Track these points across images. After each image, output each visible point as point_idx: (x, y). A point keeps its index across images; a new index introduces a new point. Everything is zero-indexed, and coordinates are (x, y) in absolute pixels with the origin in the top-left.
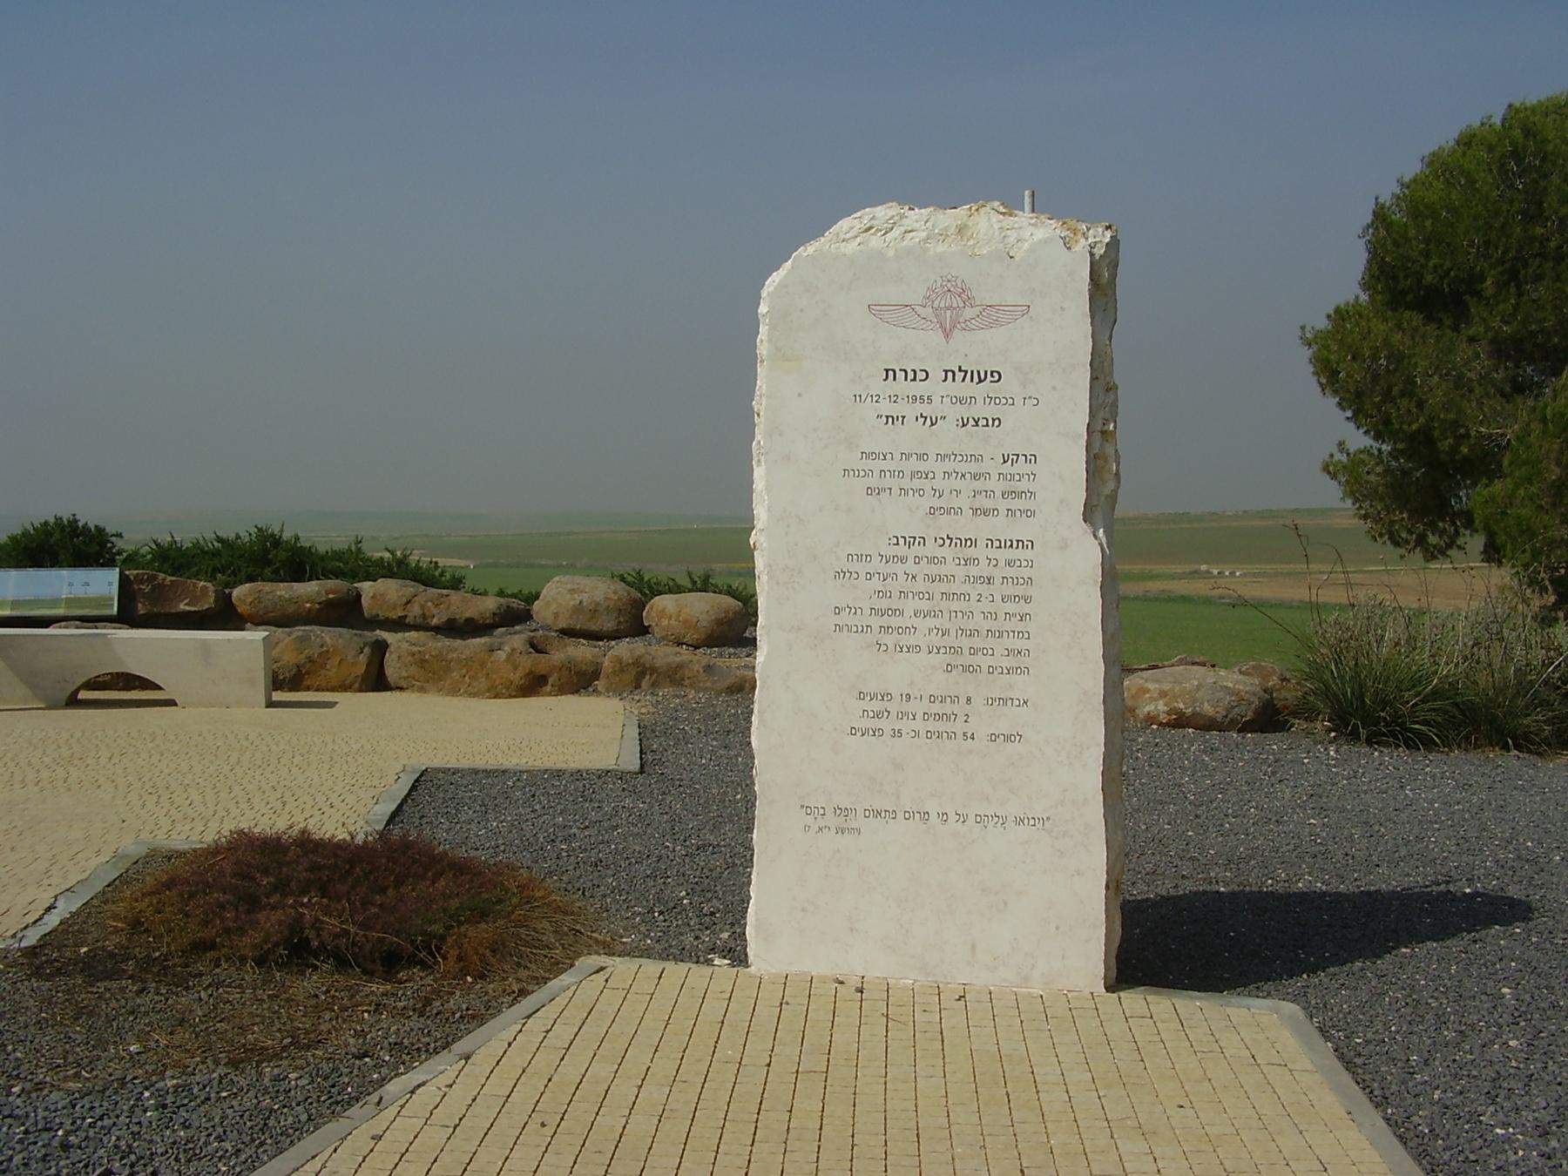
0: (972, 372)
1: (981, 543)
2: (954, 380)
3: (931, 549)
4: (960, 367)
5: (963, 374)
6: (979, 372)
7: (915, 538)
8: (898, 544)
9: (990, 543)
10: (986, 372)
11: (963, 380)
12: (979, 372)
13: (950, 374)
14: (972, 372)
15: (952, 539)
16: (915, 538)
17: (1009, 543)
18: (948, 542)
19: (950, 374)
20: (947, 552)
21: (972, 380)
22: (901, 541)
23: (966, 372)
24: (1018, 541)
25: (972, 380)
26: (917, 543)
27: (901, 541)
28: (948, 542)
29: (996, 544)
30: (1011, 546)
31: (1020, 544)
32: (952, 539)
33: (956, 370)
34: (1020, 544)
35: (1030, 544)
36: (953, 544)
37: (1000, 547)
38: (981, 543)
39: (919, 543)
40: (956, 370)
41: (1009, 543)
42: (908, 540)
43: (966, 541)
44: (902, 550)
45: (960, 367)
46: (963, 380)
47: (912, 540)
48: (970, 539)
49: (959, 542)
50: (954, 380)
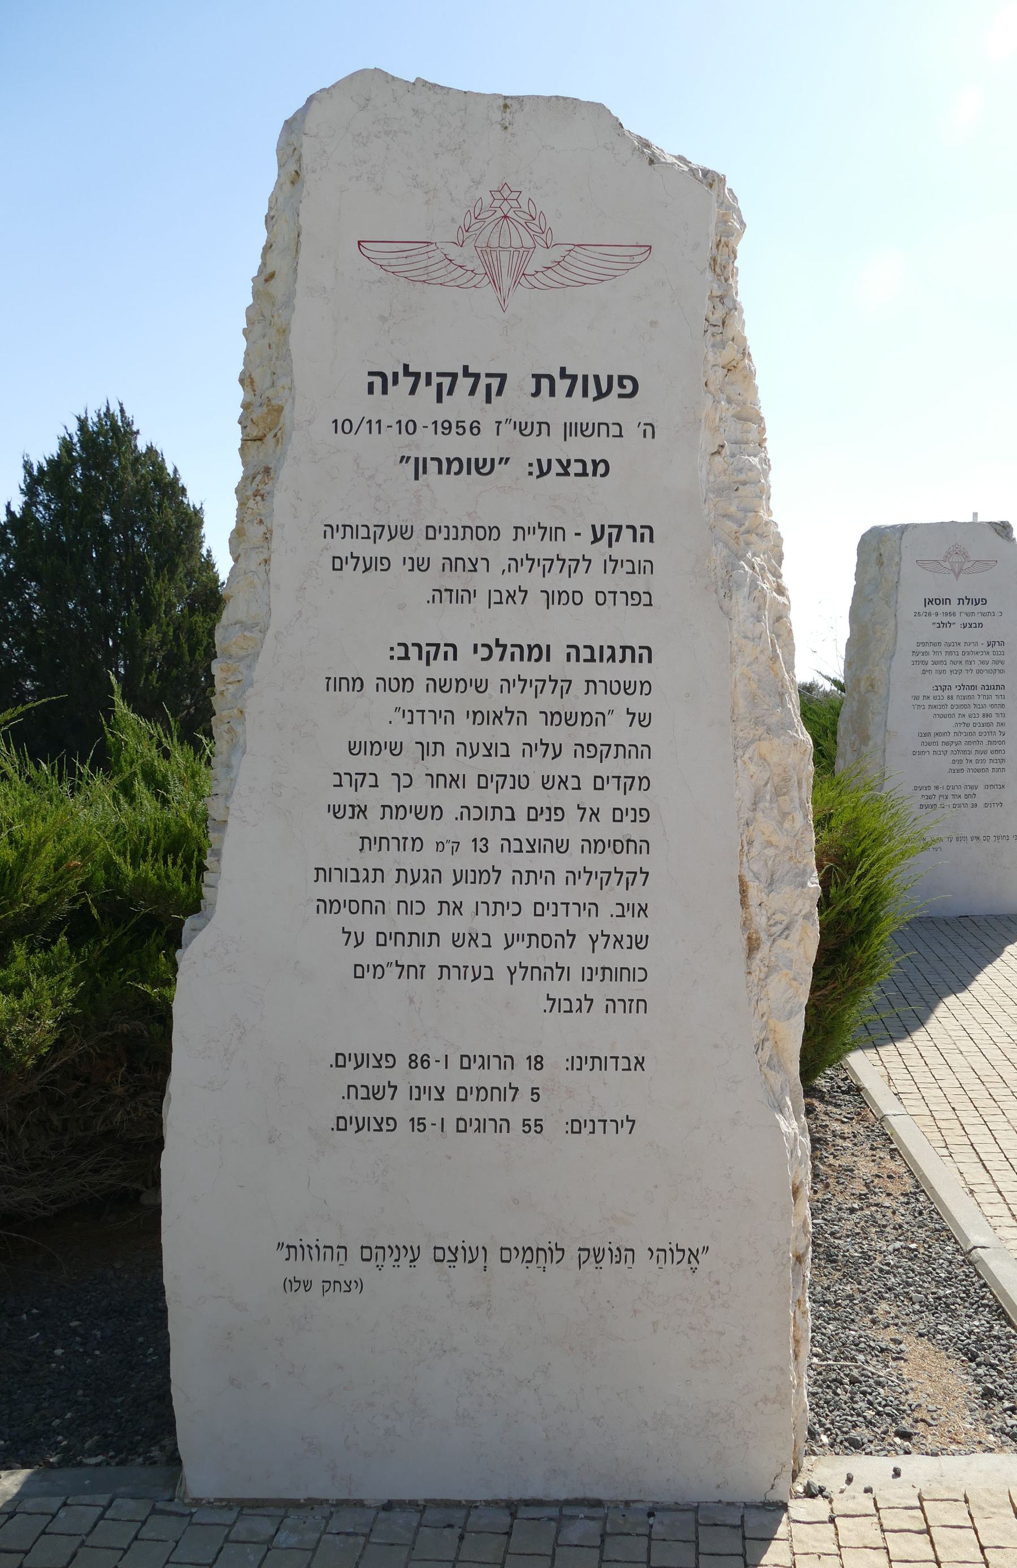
0: (585, 378)
1: (558, 653)
2: (552, 393)
3: (467, 666)
4: (563, 370)
5: (568, 382)
6: (597, 378)
7: (438, 646)
8: (407, 657)
9: (573, 652)
10: (610, 378)
11: (570, 394)
12: (597, 378)
13: (545, 383)
14: (585, 378)
15: (505, 646)
16: (438, 646)
17: (607, 653)
18: (497, 652)
19: (545, 383)
20: (498, 670)
21: (585, 394)
22: (413, 652)
23: (574, 378)
24: (624, 648)
25: (585, 394)
26: (441, 655)
27: (413, 652)
28: (497, 652)
29: (585, 654)
30: (612, 657)
31: (628, 652)
32: (505, 646)
33: (556, 375)
34: (628, 652)
35: (645, 652)
36: (508, 655)
37: (592, 660)
38: (558, 653)
39: (446, 653)
40: (556, 375)
41: (607, 653)
42: (425, 649)
43: (531, 649)
44: (415, 668)
45: (563, 370)
46: (570, 394)
47: (433, 649)
48: (538, 646)
49: (517, 651)
50: (552, 393)
